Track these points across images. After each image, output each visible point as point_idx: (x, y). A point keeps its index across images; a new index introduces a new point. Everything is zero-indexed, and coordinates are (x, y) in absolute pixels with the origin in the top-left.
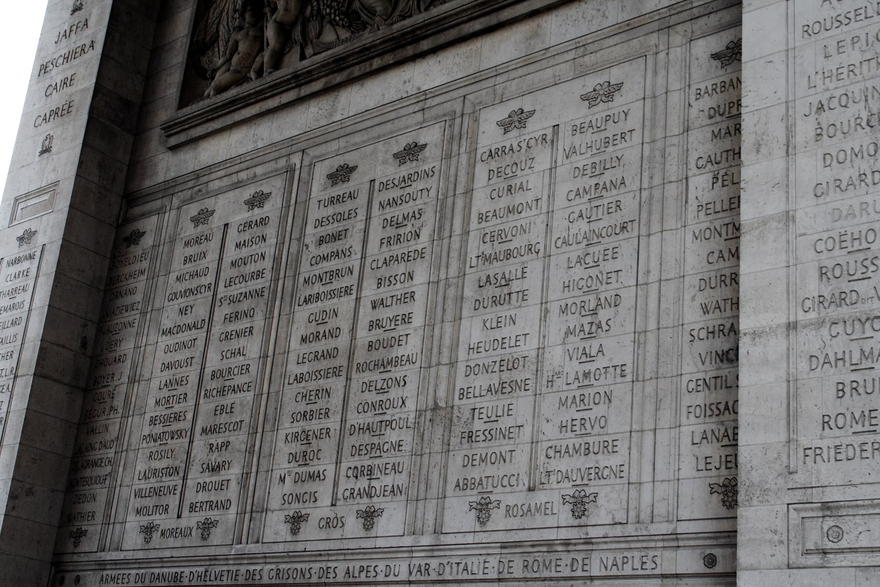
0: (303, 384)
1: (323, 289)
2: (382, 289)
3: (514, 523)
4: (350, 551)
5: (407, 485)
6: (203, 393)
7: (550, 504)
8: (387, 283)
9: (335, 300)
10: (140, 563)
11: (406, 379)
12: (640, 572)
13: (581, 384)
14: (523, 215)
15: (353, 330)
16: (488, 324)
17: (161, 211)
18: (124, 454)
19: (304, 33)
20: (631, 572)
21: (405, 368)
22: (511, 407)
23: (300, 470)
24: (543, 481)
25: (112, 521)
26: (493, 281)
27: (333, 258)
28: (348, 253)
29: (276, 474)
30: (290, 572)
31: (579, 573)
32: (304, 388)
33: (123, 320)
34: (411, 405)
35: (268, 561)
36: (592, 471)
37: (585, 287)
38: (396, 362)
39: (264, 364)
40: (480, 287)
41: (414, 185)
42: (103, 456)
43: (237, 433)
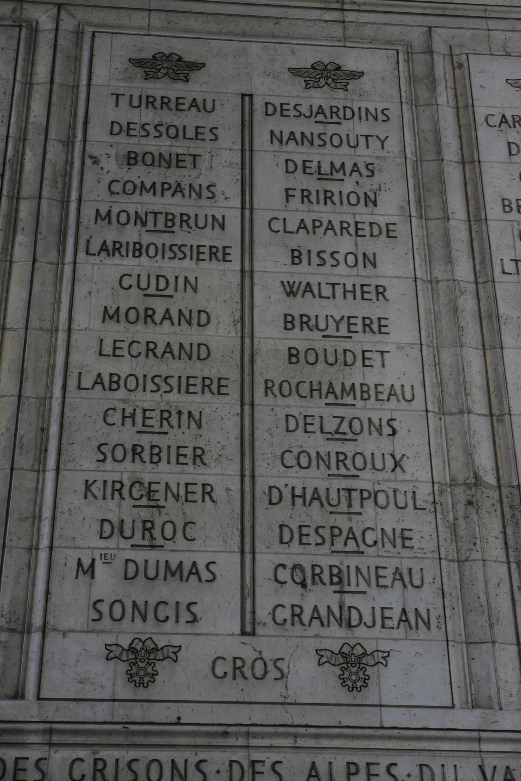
1: (146, 239)
2: (303, 267)
4: (311, 730)
5: (440, 611)
9: (187, 263)
11: (395, 424)
27: (168, 193)
28: (205, 193)
30: (140, 768)
32: (125, 401)
35: (55, 739)
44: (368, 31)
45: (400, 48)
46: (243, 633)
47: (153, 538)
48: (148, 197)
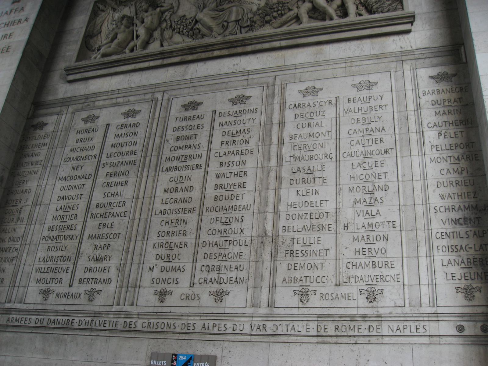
1: (179, 164)
2: (223, 168)
4: (205, 314)
5: (247, 278)
6: (89, 215)
7: (351, 294)
8: (227, 165)
9: (189, 171)
10: (39, 312)
11: (243, 218)
12: (415, 334)
13: (367, 230)
14: (320, 138)
16: (300, 193)
19: (162, 35)
20: (409, 334)
21: (241, 212)
22: (319, 239)
23: (165, 265)
25: (17, 284)
27: (187, 148)
28: (198, 147)
29: (147, 266)
30: (159, 324)
31: (374, 333)
32: (167, 218)
33: (29, 170)
35: (140, 317)
36: (379, 277)
37: (364, 178)
38: (236, 208)
39: (136, 203)
40: (293, 173)
41: (244, 116)
42: (11, 246)
43: (116, 240)
44: (255, 81)
45: (264, 85)
46: (190, 287)
47: (169, 259)
48: (181, 151)
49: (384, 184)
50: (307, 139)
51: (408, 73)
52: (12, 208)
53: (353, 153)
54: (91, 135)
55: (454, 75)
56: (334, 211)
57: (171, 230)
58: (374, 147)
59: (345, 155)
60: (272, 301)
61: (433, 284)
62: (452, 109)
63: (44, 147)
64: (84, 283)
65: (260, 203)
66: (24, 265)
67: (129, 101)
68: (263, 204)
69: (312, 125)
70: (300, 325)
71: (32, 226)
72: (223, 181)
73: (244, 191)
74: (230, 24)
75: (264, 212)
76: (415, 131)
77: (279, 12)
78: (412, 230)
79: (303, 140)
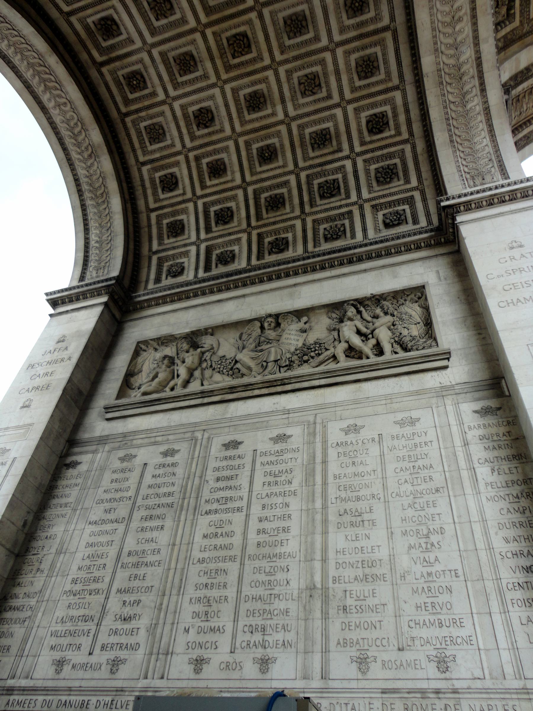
0: (205, 565)
1: (219, 507)
2: (265, 511)
3: (389, 674)
4: (248, 690)
5: (296, 640)
6: (120, 565)
8: (270, 507)
9: (230, 514)
11: (289, 567)
13: (427, 580)
14: (365, 478)
15: (245, 534)
16: (349, 538)
17: (95, 452)
18: (44, 603)
19: (202, 374)
21: (287, 560)
23: (202, 624)
24: (409, 644)
25: (26, 653)
26: (349, 513)
28: (239, 488)
29: (181, 627)
32: (205, 567)
33: (57, 513)
34: (294, 584)
36: (448, 639)
38: (280, 556)
39: (172, 550)
41: (285, 455)
43: (147, 594)
44: (296, 420)
46: (231, 652)
49: (439, 526)
50: (352, 479)
51: (450, 408)
52: (32, 557)
53: (402, 493)
54: (127, 475)
55: (499, 409)
56: (387, 558)
57: (209, 581)
58: (424, 486)
59: (394, 495)
60: (325, 671)
61: (514, 649)
62: (502, 443)
63: (76, 488)
64: (108, 649)
65: (306, 550)
66: (38, 627)
67: (168, 440)
68: (309, 551)
69: (356, 464)
70: (362, 704)
71: (53, 579)
72: (266, 525)
73: (289, 536)
74: (270, 364)
75: (312, 560)
76: (464, 467)
77: (317, 352)
78: (478, 580)
79: (348, 479)
